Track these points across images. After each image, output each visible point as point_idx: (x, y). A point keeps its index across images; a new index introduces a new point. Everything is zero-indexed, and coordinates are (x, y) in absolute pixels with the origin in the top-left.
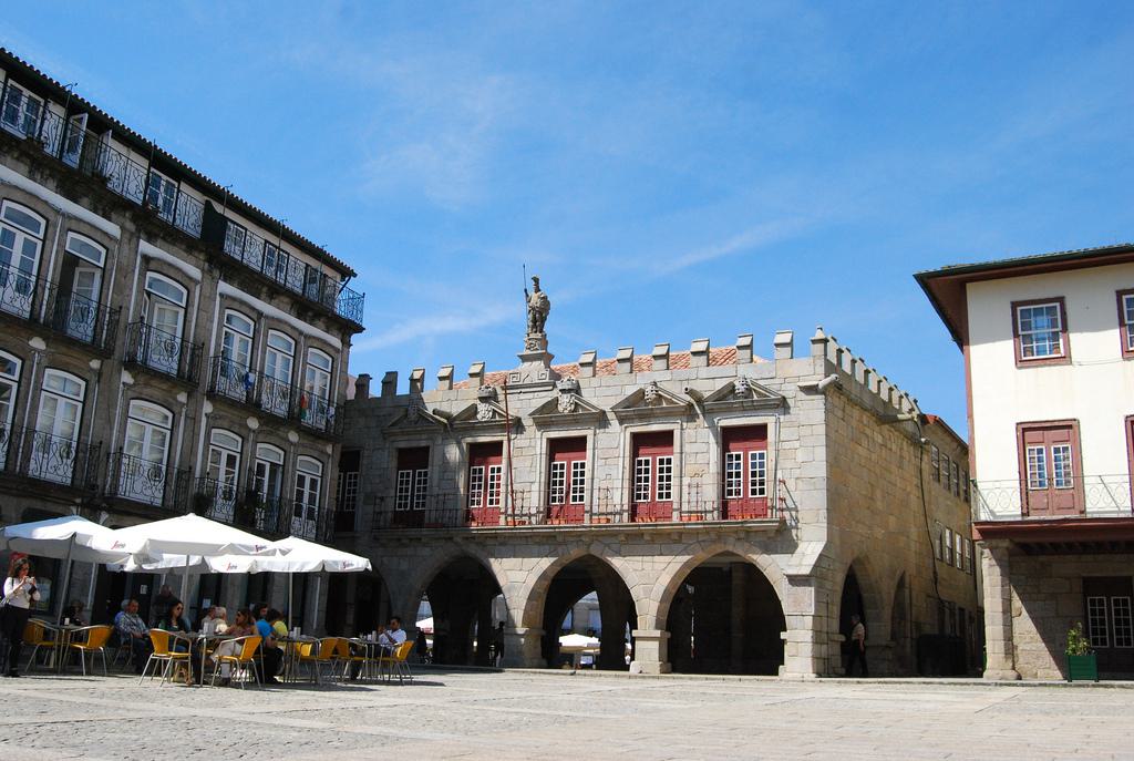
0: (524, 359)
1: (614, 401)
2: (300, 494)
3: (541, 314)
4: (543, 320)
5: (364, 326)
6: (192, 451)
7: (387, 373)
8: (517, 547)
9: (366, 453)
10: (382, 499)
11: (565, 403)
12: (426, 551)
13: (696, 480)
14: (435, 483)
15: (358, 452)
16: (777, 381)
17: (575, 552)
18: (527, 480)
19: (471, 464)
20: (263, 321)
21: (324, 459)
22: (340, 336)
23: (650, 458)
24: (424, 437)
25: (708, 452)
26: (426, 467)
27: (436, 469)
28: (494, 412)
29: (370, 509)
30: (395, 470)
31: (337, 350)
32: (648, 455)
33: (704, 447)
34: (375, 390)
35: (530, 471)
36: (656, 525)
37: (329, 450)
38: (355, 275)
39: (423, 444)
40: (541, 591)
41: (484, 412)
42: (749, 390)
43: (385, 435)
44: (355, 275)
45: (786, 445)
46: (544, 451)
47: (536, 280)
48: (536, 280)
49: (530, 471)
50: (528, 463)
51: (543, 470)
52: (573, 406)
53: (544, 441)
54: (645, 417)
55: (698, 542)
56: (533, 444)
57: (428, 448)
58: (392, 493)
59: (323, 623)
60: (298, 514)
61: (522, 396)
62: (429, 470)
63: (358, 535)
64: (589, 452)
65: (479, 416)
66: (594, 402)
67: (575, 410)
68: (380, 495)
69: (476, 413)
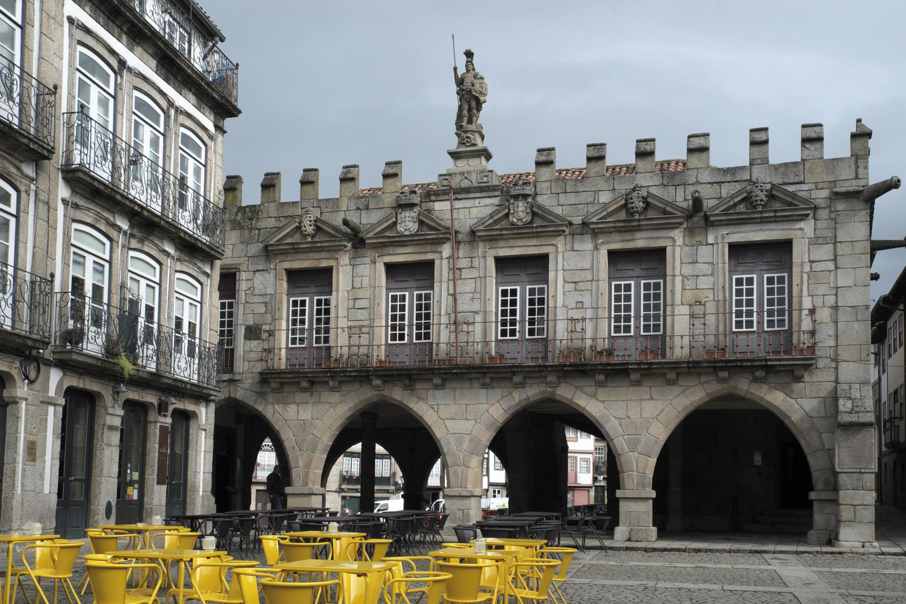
1: (583, 210)
6: (49, 254)
7: (267, 175)
8: (458, 391)
9: (244, 276)
10: (271, 333)
12: (335, 397)
13: (698, 310)
14: (342, 312)
15: (234, 275)
16: (805, 187)
22: (212, 117)
23: (632, 283)
26: (330, 293)
29: (254, 344)
30: (285, 298)
32: (631, 278)
33: (707, 269)
34: (251, 195)
39: (324, 264)
42: (771, 196)
45: (817, 267)
47: (469, 54)
48: (469, 54)
54: (628, 227)
58: (284, 326)
59: (210, 489)
63: (237, 377)
64: (551, 275)
65: (401, 228)
66: (558, 211)
67: (531, 222)
68: (267, 328)
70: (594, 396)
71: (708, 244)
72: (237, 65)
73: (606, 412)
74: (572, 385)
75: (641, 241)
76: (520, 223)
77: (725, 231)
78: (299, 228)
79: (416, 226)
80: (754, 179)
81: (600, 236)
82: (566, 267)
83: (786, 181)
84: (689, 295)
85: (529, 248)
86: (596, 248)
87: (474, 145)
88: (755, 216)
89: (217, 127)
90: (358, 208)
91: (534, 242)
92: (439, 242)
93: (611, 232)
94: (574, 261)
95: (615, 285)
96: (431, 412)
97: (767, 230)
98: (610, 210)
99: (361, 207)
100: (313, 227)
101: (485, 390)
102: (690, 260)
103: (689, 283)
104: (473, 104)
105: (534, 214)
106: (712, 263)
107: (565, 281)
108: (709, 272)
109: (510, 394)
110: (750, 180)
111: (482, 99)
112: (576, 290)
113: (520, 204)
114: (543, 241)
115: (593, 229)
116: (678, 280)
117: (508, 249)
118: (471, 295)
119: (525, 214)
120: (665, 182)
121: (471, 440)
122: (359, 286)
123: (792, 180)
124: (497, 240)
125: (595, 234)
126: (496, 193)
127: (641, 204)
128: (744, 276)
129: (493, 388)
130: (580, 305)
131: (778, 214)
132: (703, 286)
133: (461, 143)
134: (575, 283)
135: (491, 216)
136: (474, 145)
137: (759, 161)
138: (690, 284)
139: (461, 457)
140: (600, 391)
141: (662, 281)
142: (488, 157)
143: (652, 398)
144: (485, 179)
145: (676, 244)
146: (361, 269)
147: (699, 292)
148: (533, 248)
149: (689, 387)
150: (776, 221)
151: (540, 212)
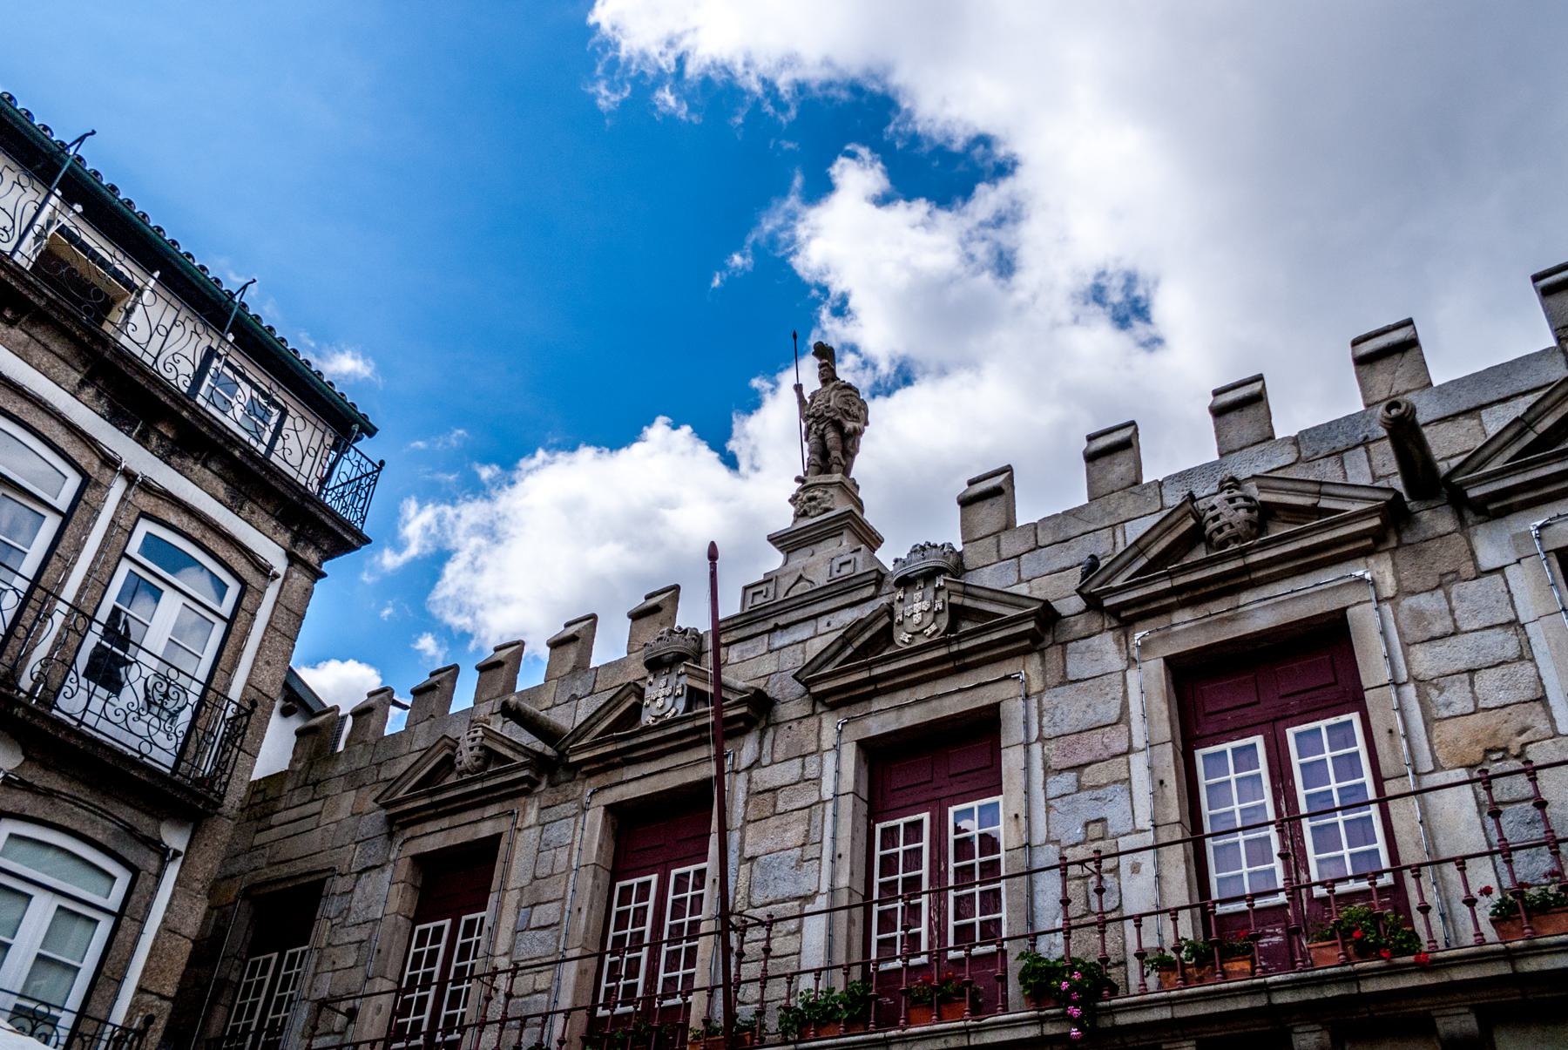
3: (838, 426)
4: (850, 442)
11: (918, 612)
18: (787, 889)
19: (617, 873)
21: (153, 863)
23: (1258, 740)
24: (492, 810)
25: (1525, 655)
27: (512, 898)
28: (694, 696)
31: (265, 571)
35: (801, 861)
36: (1356, 977)
37: (176, 839)
38: (371, 431)
41: (662, 699)
43: (398, 822)
44: (371, 431)
46: (848, 783)
49: (801, 861)
50: (794, 835)
51: (844, 846)
52: (944, 621)
53: (849, 753)
56: (811, 771)
57: (497, 838)
61: (780, 640)
62: (487, 915)
64: (1012, 760)
65: (647, 719)
67: (952, 627)
69: (636, 711)
71: (1481, 574)
72: (382, 463)
75: (1261, 612)
76: (920, 641)
77: (1532, 522)
78: (448, 763)
79: (681, 704)
81: (1138, 625)
82: (1047, 732)
84: (1461, 735)
85: (947, 701)
86: (1132, 662)
89: (292, 558)
90: (574, 697)
91: (967, 680)
92: (730, 730)
93: (1167, 610)
94: (1069, 709)
98: (1155, 551)
99: (579, 694)
100: (476, 751)
104: (831, 435)
105: (957, 613)
106: (1515, 624)
107: (1048, 770)
108: (1511, 650)
111: (849, 425)
113: (918, 595)
114: (985, 674)
115: (1114, 612)
117: (893, 715)
118: (798, 852)
119: (929, 617)
122: (547, 871)
124: (868, 697)
125: (1123, 620)
126: (871, 590)
127: (1242, 512)
130: (1095, 831)
132: (1503, 697)
133: (799, 515)
135: (845, 640)
136: (827, 510)
141: (1355, 717)
142: (871, 540)
144: (846, 570)
145: (1374, 601)
146: (553, 833)
147: (1494, 719)
148: (956, 698)
151: (968, 602)
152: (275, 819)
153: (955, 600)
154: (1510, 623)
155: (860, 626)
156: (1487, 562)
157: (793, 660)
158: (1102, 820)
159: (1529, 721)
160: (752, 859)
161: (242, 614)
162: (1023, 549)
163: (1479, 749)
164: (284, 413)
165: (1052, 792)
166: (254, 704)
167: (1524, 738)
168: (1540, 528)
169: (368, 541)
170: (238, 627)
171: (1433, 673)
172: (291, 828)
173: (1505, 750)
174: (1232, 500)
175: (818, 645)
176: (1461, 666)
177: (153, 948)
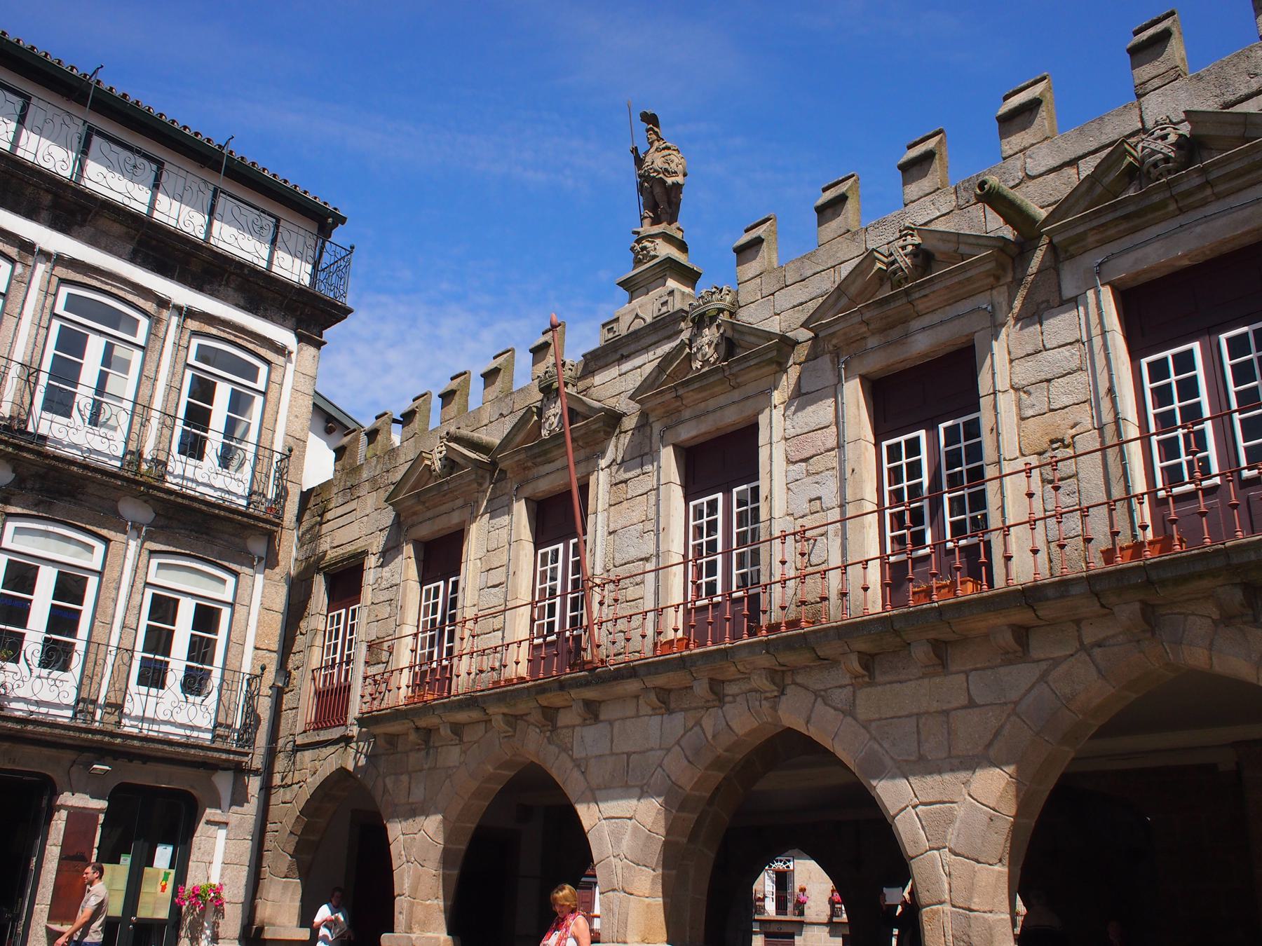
0: (632, 287)
2: (159, 641)
5: (349, 302)
17: (741, 721)
20: (41, 268)
31: (281, 350)
38: (342, 220)
40: (685, 840)
44: (342, 220)
55: (1083, 647)
60: (153, 676)
61: (626, 366)
70: (850, 712)
73: (876, 746)
74: (807, 689)
80: (1150, 124)
83: (1230, 98)
84: (1037, 432)
87: (655, 257)
88: (1156, 198)
95: (888, 447)
96: (576, 774)
97: (1197, 222)
101: (658, 718)
102: (1030, 349)
103: (1032, 400)
107: (790, 462)
109: (698, 723)
110: (1143, 130)
112: (809, 474)
116: (1007, 403)
120: (961, 202)
121: (635, 829)
123: (1244, 91)
128: (1168, 354)
129: (670, 712)
131: (1214, 174)
134: (805, 460)
135: (661, 368)
137: (1157, 82)
138: (1037, 401)
139: (619, 871)
140: (862, 694)
143: (971, 704)
144: (664, 309)
149: (1056, 662)
150: (1218, 197)
152: (329, 515)
153: (729, 334)
154: (1077, 341)
155: (667, 359)
156: (1068, 292)
157: (634, 380)
158: (819, 498)
159: (1078, 419)
160: (614, 532)
161: (272, 386)
162: (775, 288)
163: (1047, 439)
164: (278, 220)
165: (791, 477)
166: (291, 450)
167: (1073, 432)
168: (1100, 265)
169: (350, 311)
170: (272, 395)
171: (1025, 383)
172: (341, 522)
173: (1062, 441)
174: (903, 248)
175: (648, 369)
176: (1044, 377)
177: (258, 622)
